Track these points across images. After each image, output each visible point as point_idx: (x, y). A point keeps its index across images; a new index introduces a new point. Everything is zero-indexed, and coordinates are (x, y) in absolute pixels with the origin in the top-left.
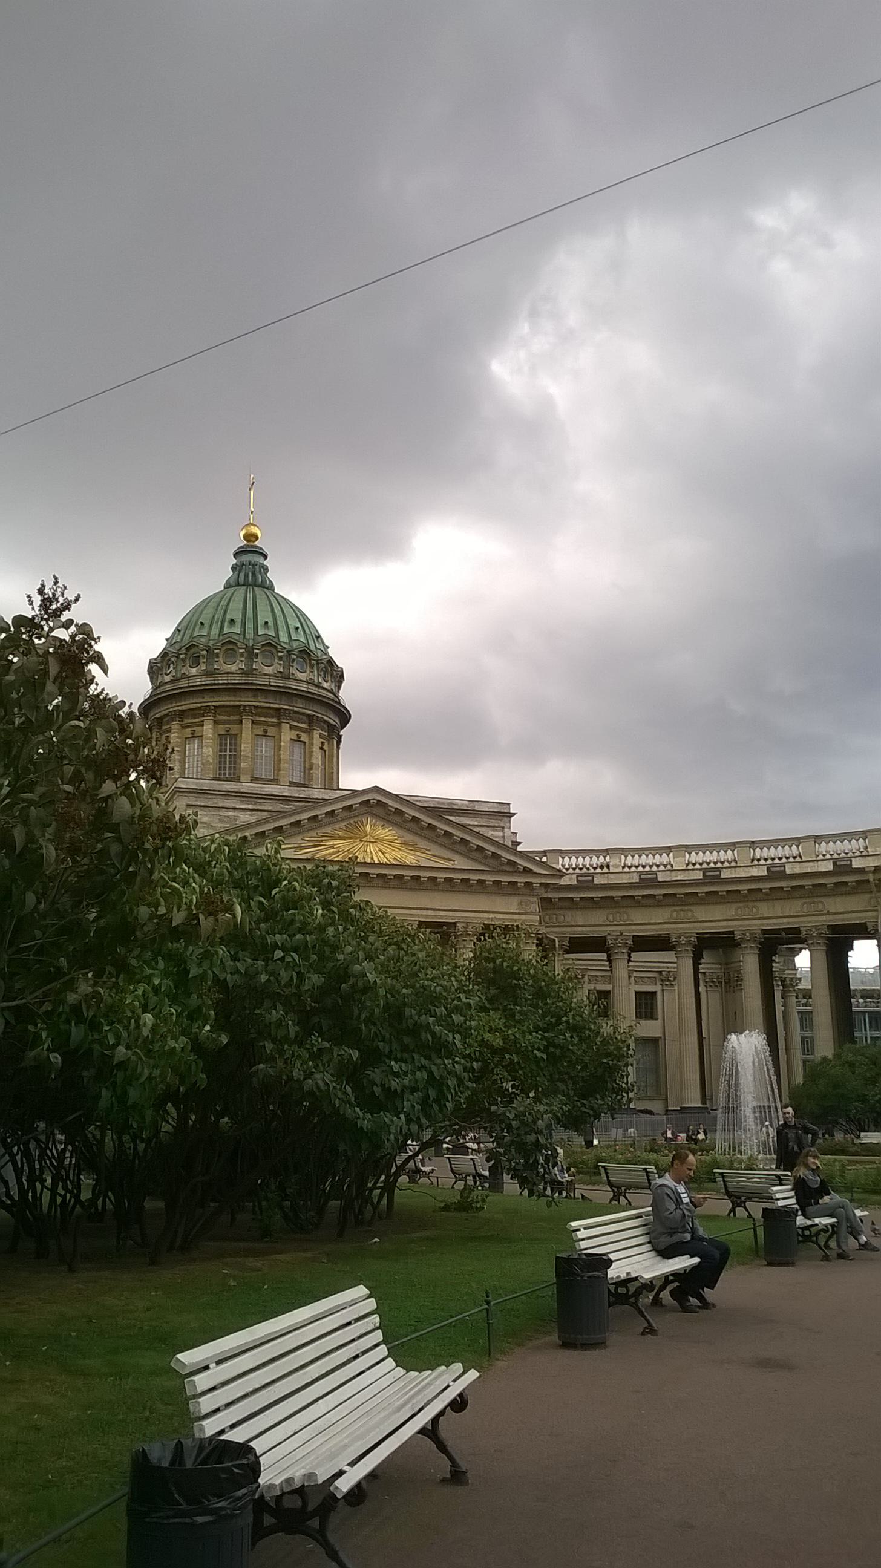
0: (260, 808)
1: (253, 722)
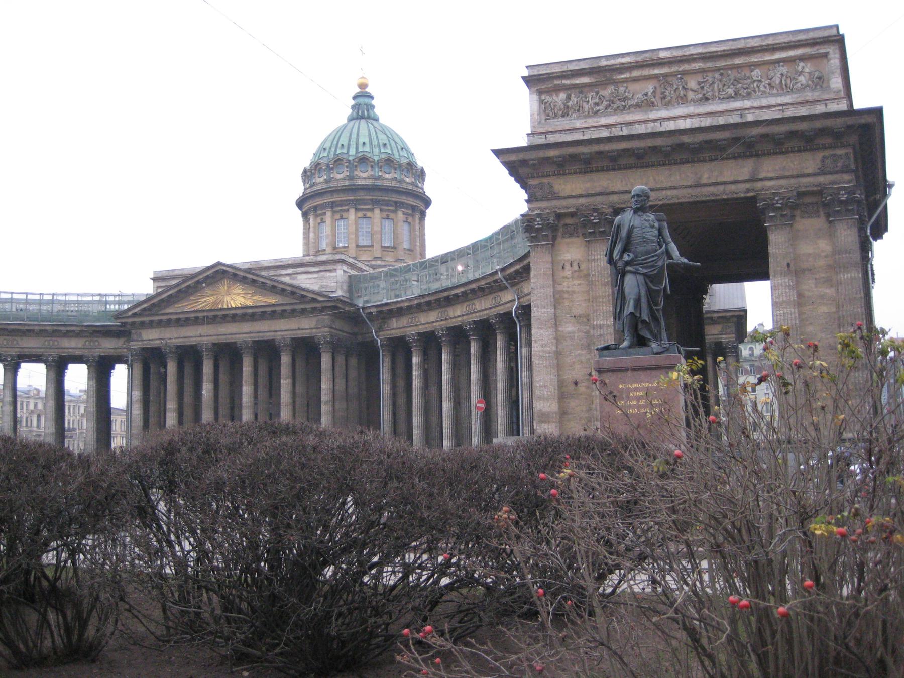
1: (334, 213)
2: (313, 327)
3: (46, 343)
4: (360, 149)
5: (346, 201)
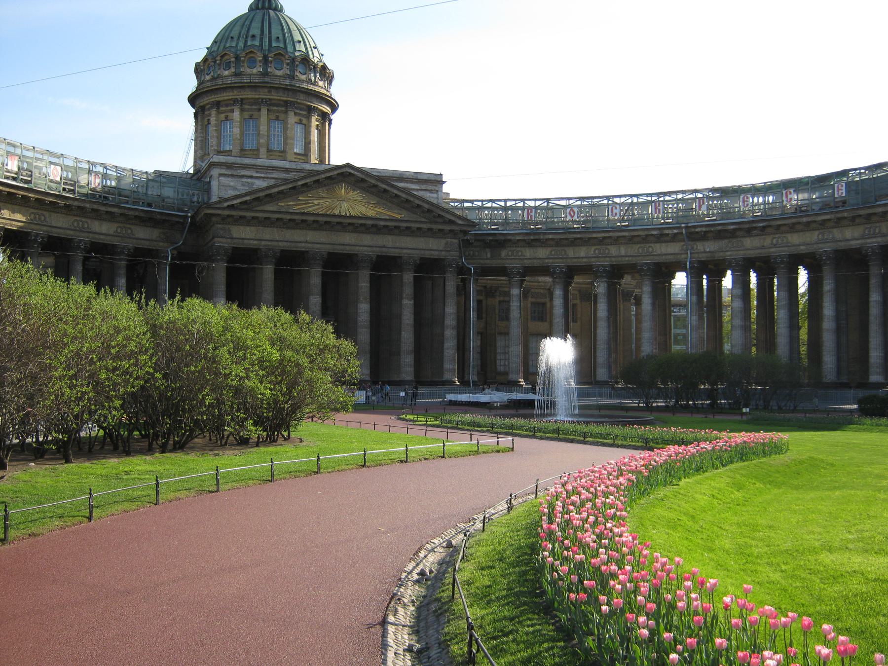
0: (269, 176)
1: (268, 110)
2: (441, 249)
5: (286, 102)
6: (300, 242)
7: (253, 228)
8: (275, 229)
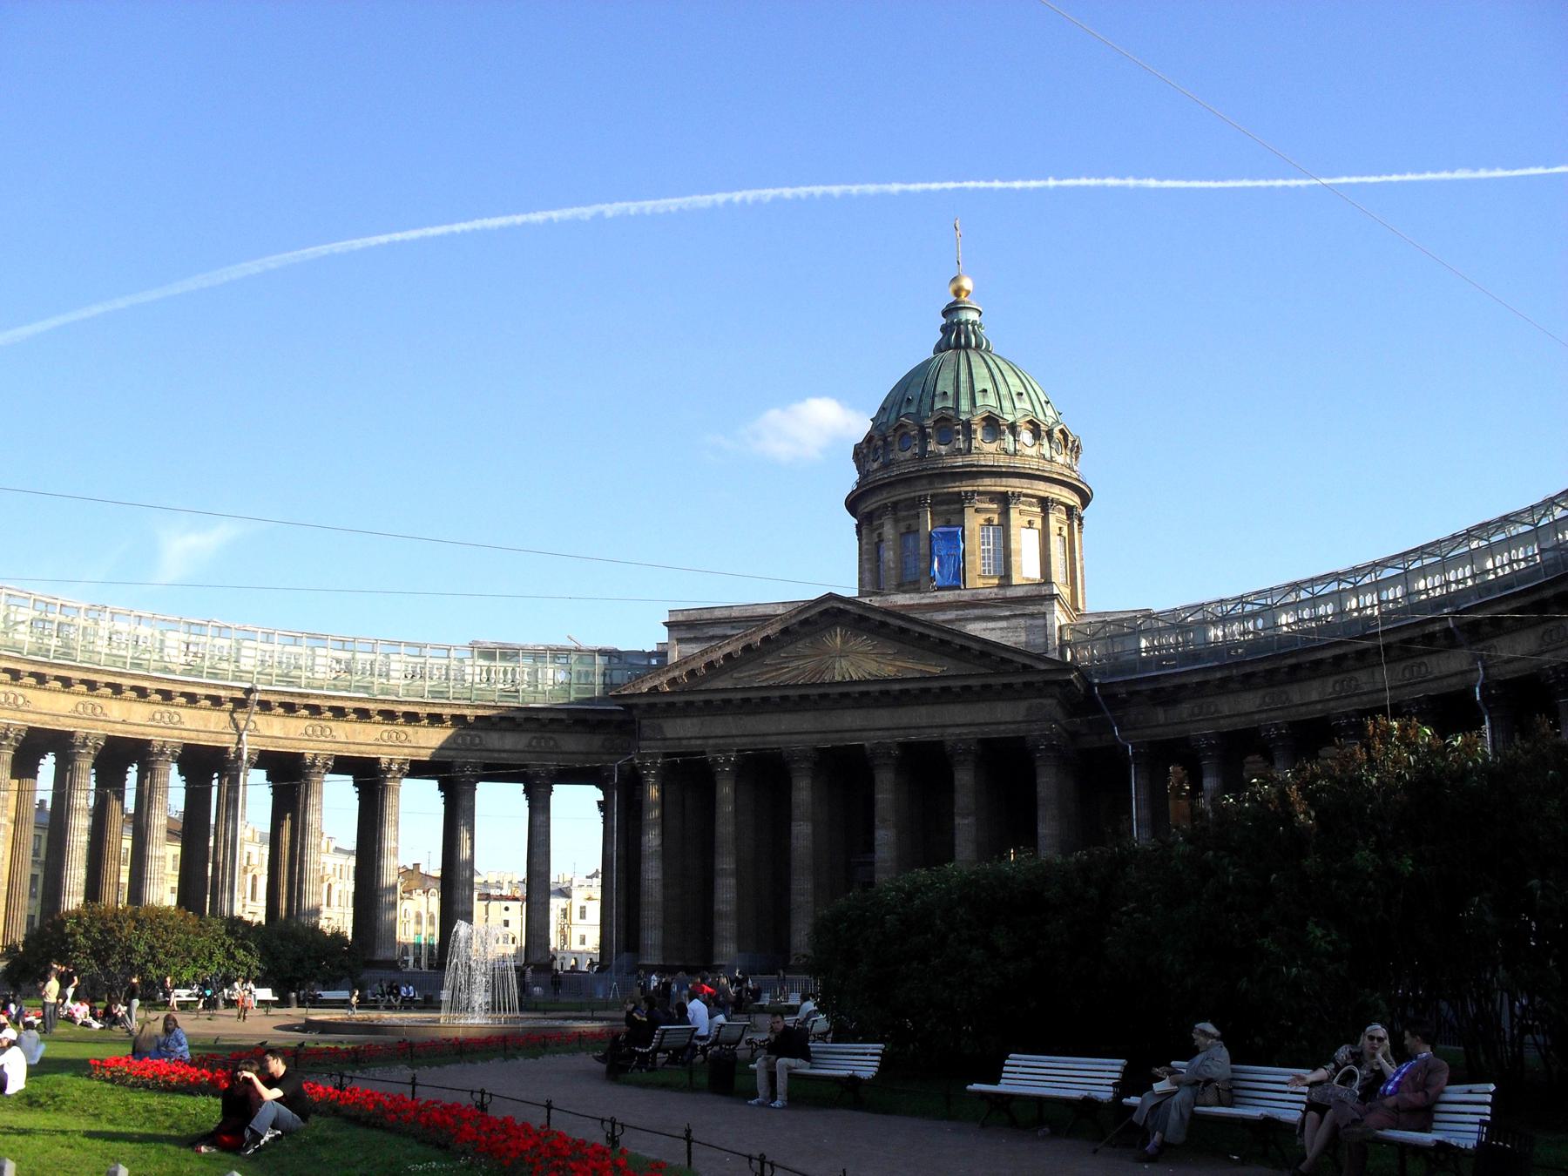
2: (1020, 719)
3: (460, 741)
4: (979, 402)
6: (768, 735)
7: (695, 720)
8: (730, 718)
